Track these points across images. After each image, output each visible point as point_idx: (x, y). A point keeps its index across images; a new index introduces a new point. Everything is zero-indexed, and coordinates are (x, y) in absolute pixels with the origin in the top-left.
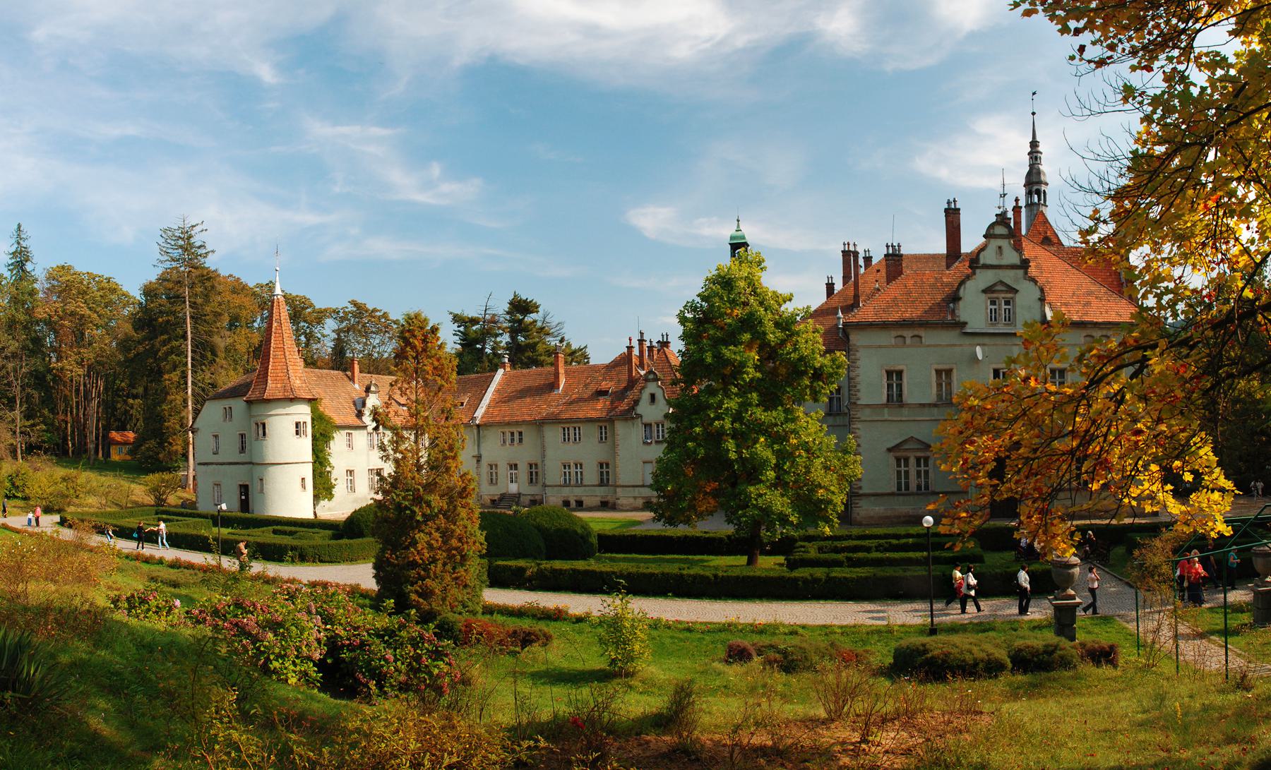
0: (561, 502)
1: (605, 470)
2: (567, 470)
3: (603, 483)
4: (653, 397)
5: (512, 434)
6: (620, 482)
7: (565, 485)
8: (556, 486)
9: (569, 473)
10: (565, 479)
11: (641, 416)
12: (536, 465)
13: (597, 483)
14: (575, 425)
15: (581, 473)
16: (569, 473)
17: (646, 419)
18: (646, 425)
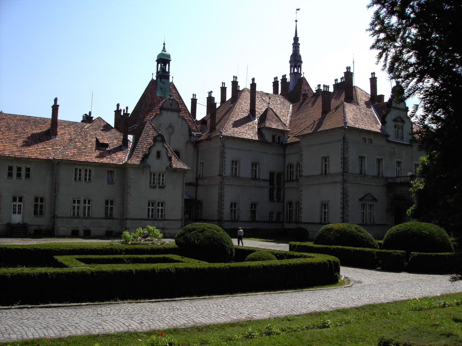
0: (71, 231)
1: (109, 206)
2: (76, 205)
3: (108, 216)
5: (19, 169)
6: (130, 216)
7: (75, 217)
8: (67, 218)
9: (78, 207)
10: (74, 213)
12: (42, 200)
13: (104, 216)
14: (86, 168)
15: (89, 207)
16: (78, 207)
17: (152, 170)
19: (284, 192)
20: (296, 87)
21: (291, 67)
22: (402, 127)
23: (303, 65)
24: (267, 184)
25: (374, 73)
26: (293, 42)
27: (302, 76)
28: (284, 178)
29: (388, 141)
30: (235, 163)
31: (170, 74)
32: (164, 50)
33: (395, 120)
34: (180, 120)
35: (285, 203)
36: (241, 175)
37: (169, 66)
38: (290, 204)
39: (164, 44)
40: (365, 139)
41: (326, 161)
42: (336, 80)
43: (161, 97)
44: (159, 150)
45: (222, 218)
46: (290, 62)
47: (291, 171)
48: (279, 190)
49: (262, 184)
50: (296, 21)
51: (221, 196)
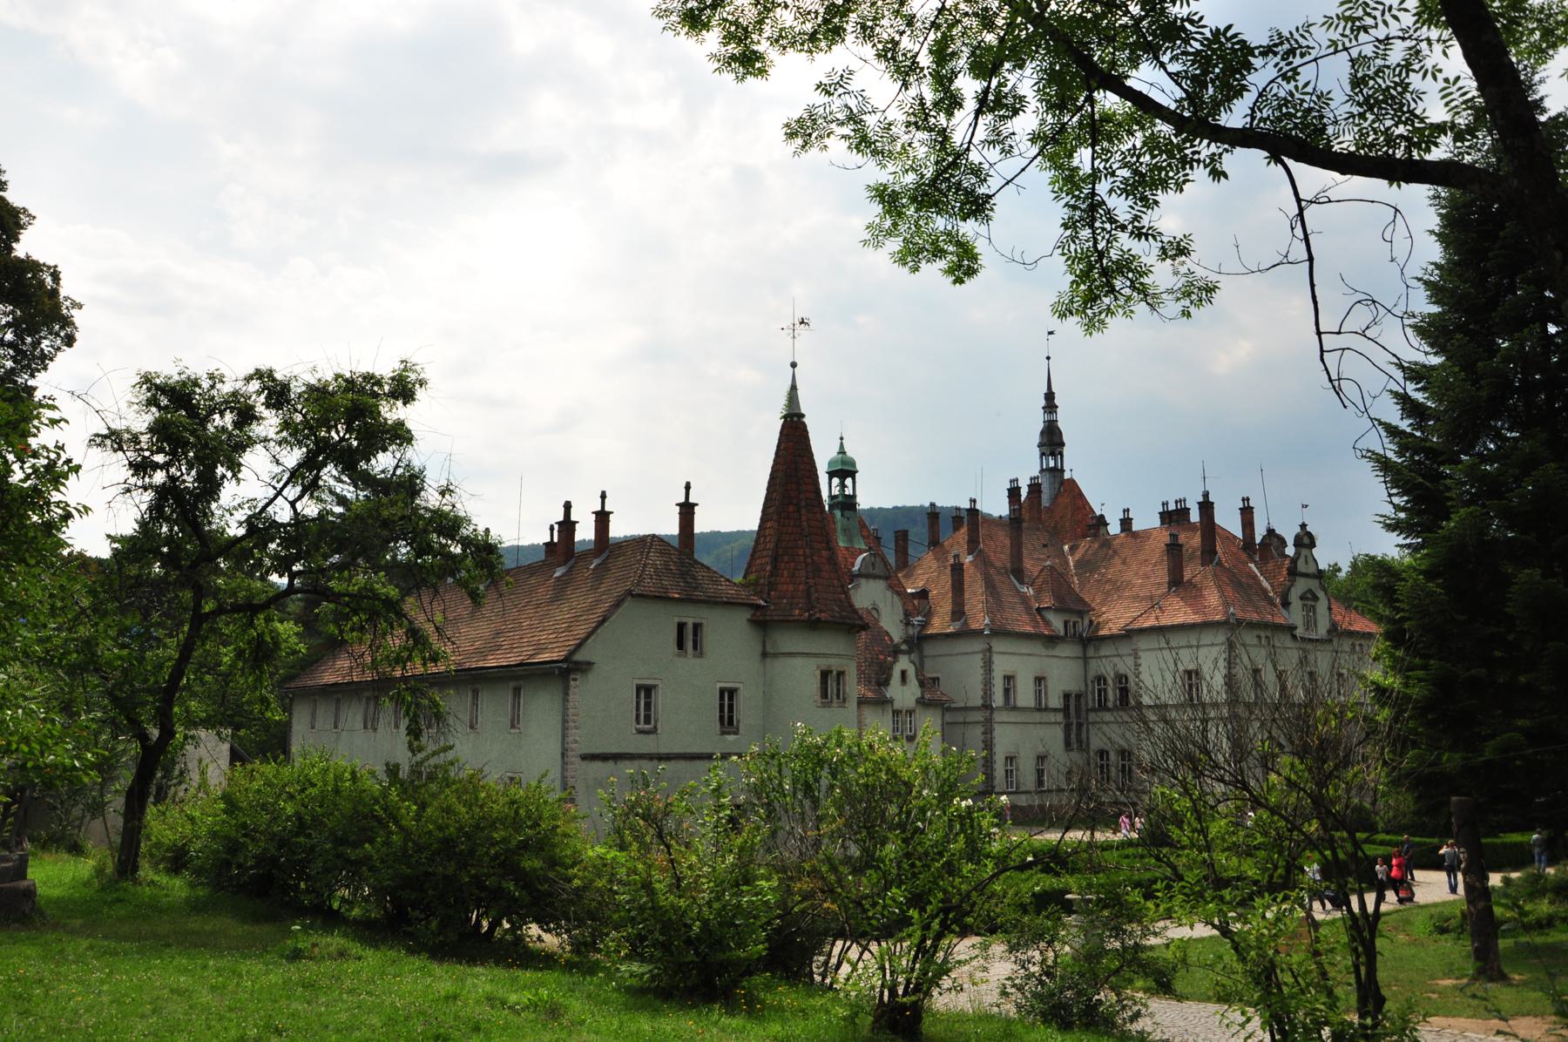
4: (904, 673)
11: (891, 702)
17: (897, 705)
18: (894, 712)
19: (1088, 731)
20: (1056, 497)
21: (1042, 454)
22: (1314, 607)
23: (1066, 450)
24: (1060, 717)
25: (1248, 499)
26: (1043, 403)
27: (1067, 476)
28: (1087, 703)
29: (1294, 637)
30: (1009, 679)
31: (858, 500)
32: (842, 452)
33: (1302, 598)
34: (889, 593)
35: (1092, 754)
36: (1020, 704)
37: (854, 483)
38: (1103, 753)
39: (842, 439)
40: (1259, 637)
41: (1190, 678)
42: (1165, 504)
43: (847, 549)
44: (904, 667)
45: (993, 787)
46: (1040, 446)
47: (1099, 690)
48: (1080, 725)
49: (1052, 717)
50: (1048, 358)
51: (988, 745)
